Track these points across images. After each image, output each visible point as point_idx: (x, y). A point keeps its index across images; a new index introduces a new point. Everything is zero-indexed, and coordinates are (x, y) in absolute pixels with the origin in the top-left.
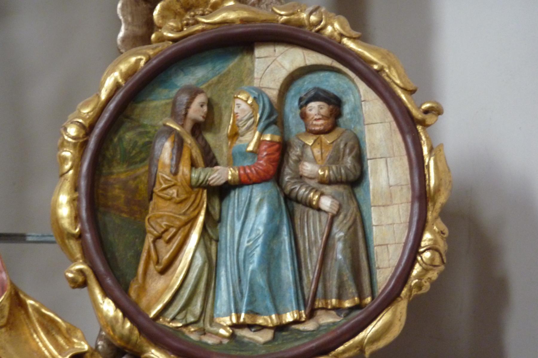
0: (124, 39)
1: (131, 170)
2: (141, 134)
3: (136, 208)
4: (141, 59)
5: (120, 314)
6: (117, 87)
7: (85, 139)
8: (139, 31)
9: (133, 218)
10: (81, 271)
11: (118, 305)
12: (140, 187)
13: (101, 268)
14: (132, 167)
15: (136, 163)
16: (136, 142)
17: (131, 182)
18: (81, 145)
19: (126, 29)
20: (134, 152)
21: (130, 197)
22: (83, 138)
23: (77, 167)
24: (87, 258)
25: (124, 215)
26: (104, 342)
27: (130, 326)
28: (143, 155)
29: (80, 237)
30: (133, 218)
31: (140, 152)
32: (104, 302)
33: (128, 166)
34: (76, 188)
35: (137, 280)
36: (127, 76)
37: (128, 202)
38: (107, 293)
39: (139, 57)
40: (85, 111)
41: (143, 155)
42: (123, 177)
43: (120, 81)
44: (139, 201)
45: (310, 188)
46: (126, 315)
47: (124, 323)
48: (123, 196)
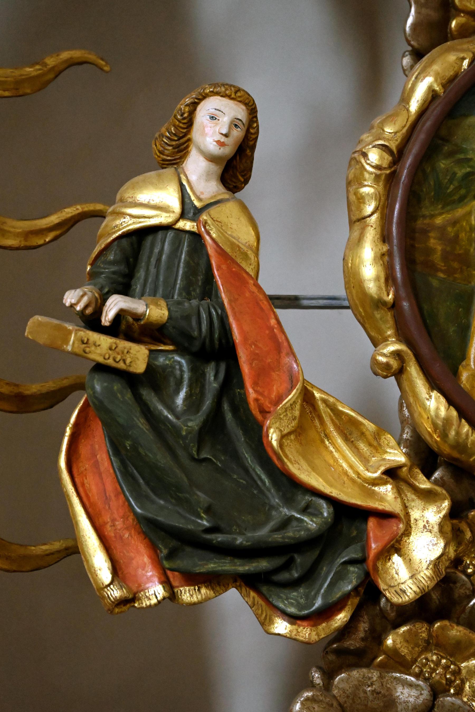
0: (415, 26)
1: (448, 212)
2: (461, 162)
3: (456, 265)
4: (464, 59)
5: (454, 413)
6: (432, 96)
7: (393, 169)
8: (434, 15)
9: (451, 279)
10: (397, 355)
11: (450, 402)
12: (460, 236)
13: (425, 350)
14: (449, 208)
15: (453, 202)
16: (455, 174)
17: (450, 229)
18: (389, 179)
19: (417, 12)
20: (452, 187)
21: (448, 249)
22: (390, 167)
23: (385, 209)
24: (403, 335)
25: (441, 275)
26: (410, 450)
27: (468, 431)
28: (463, 191)
29: (394, 306)
30: (451, 279)
31: (459, 187)
32: (430, 397)
33: (443, 208)
34: (385, 237)
35: (469, 365)
36: (448, 83)
37: (446, 257)
38: (434, 384)
39: (462, 55)
40: (389, 129)
41: (463, 191)
42: (439, 221)
43: (437, 88)
44: (459, 255)
45: (245, 178)
46: (462, 414)
47: (459, 425)
48: (439, 248)
